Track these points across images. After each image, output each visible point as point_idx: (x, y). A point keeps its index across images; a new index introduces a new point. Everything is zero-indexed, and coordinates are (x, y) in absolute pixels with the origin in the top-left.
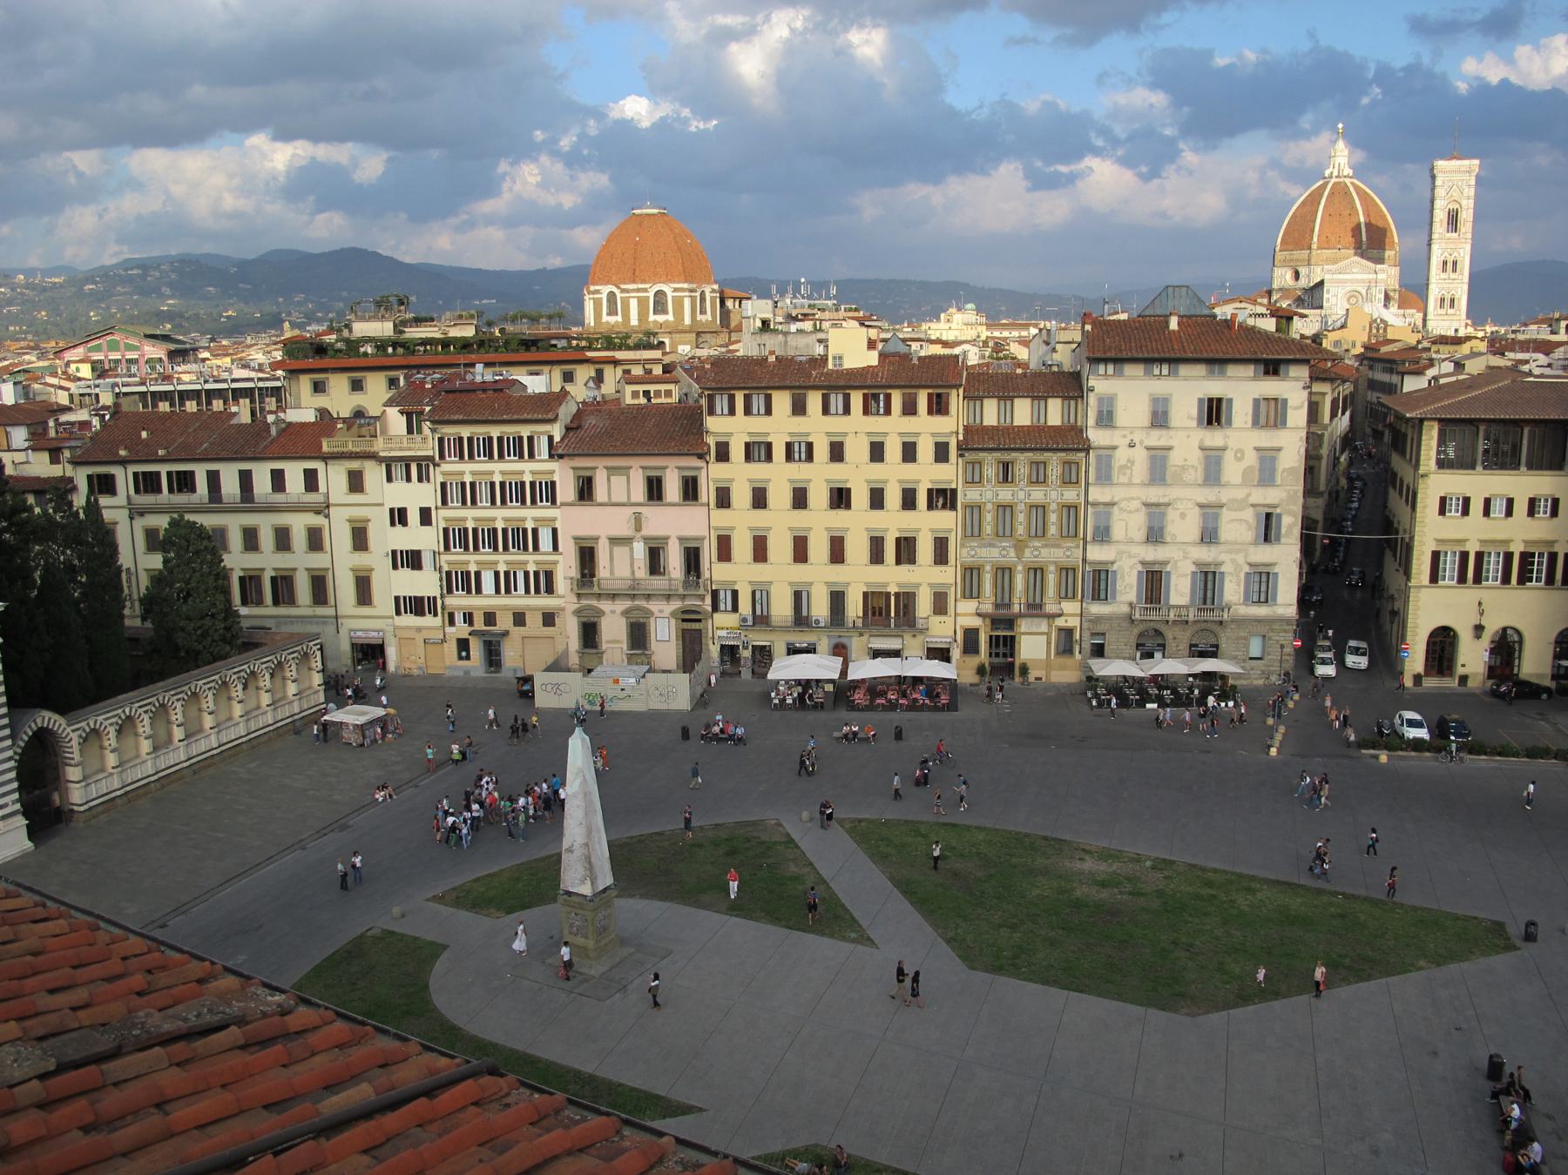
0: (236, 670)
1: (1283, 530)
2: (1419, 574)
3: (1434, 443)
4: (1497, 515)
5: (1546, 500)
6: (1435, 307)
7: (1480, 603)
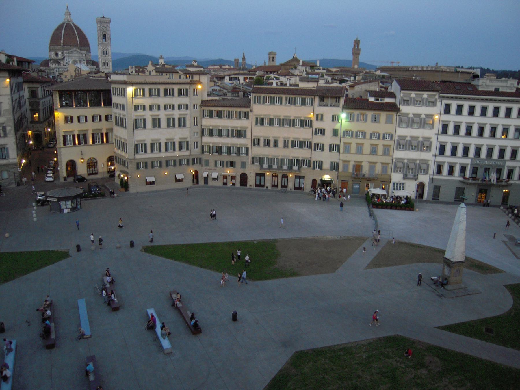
1: (8, 132)
2: (60, 143)
3: (58, 99)
4: (82, 122)
5: (97, 116)
6: (102, 65)
7: (81, 151)
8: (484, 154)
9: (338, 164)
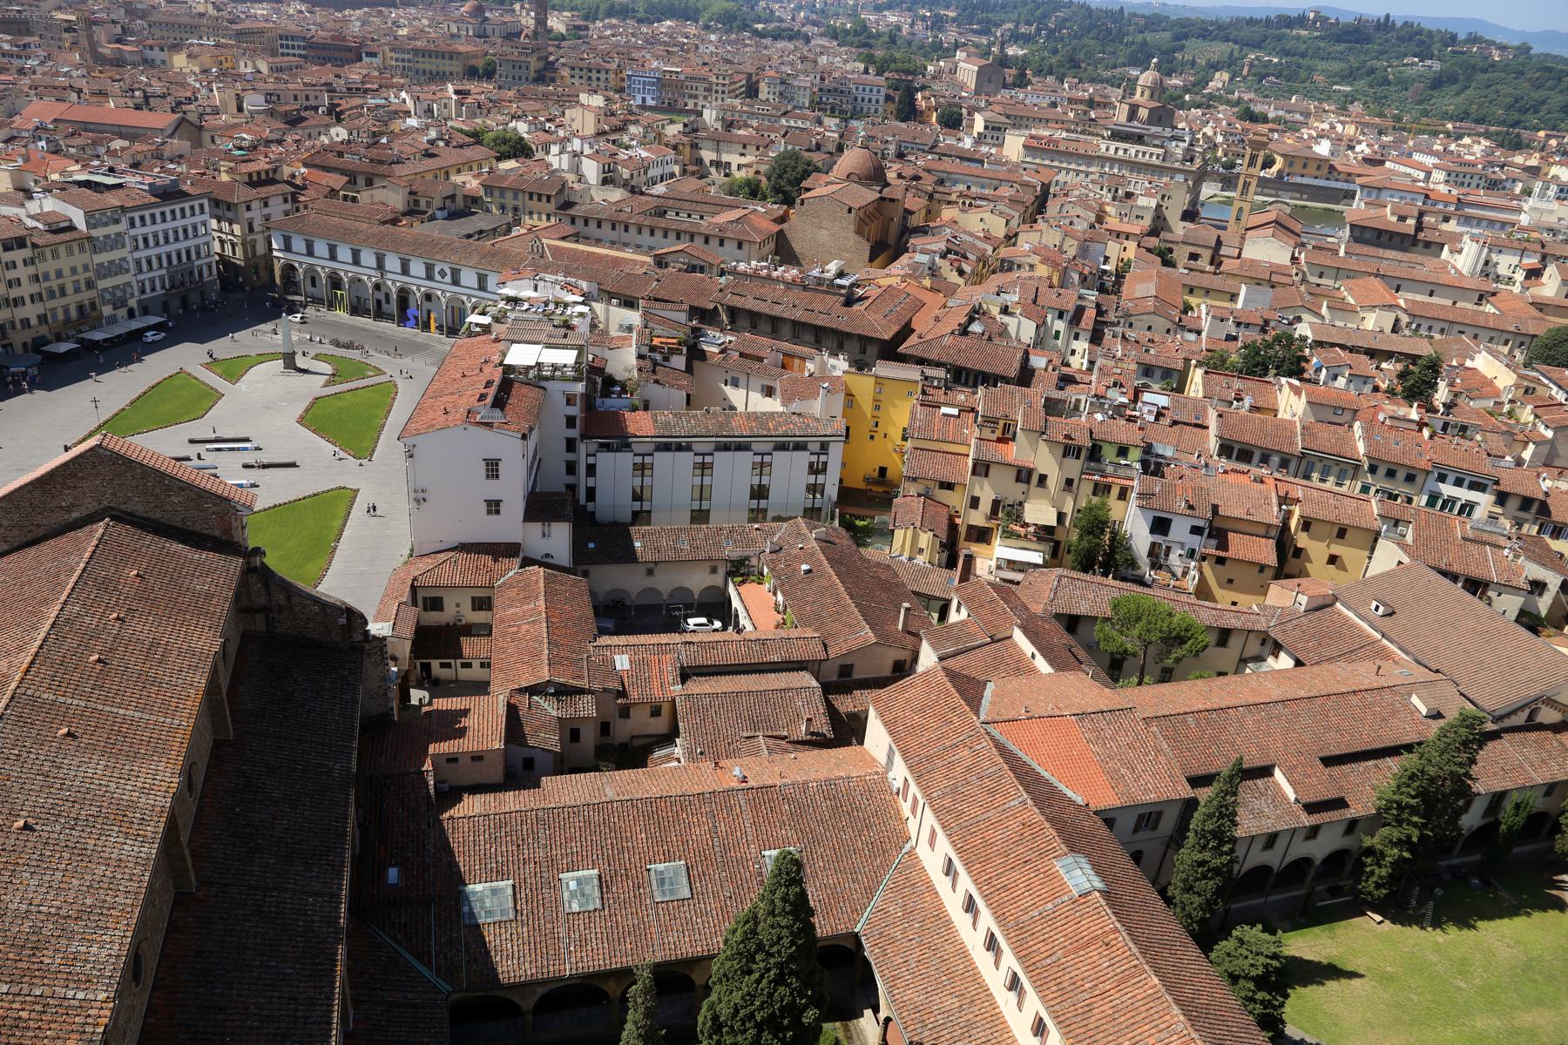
8: (175, 261)
9: (45, 315)
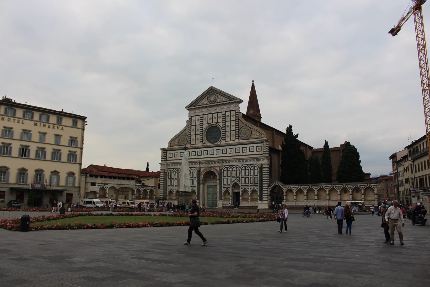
0: (338, 185)
